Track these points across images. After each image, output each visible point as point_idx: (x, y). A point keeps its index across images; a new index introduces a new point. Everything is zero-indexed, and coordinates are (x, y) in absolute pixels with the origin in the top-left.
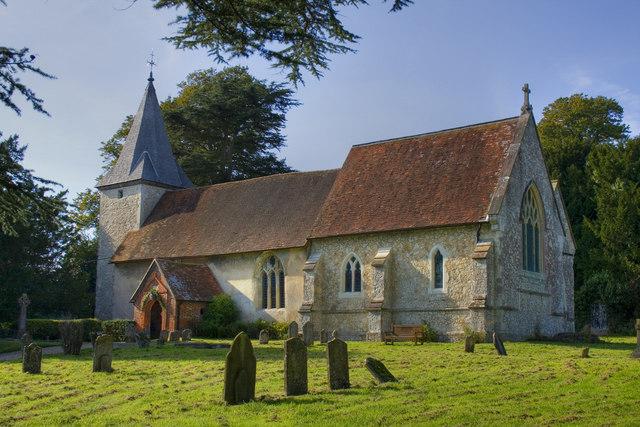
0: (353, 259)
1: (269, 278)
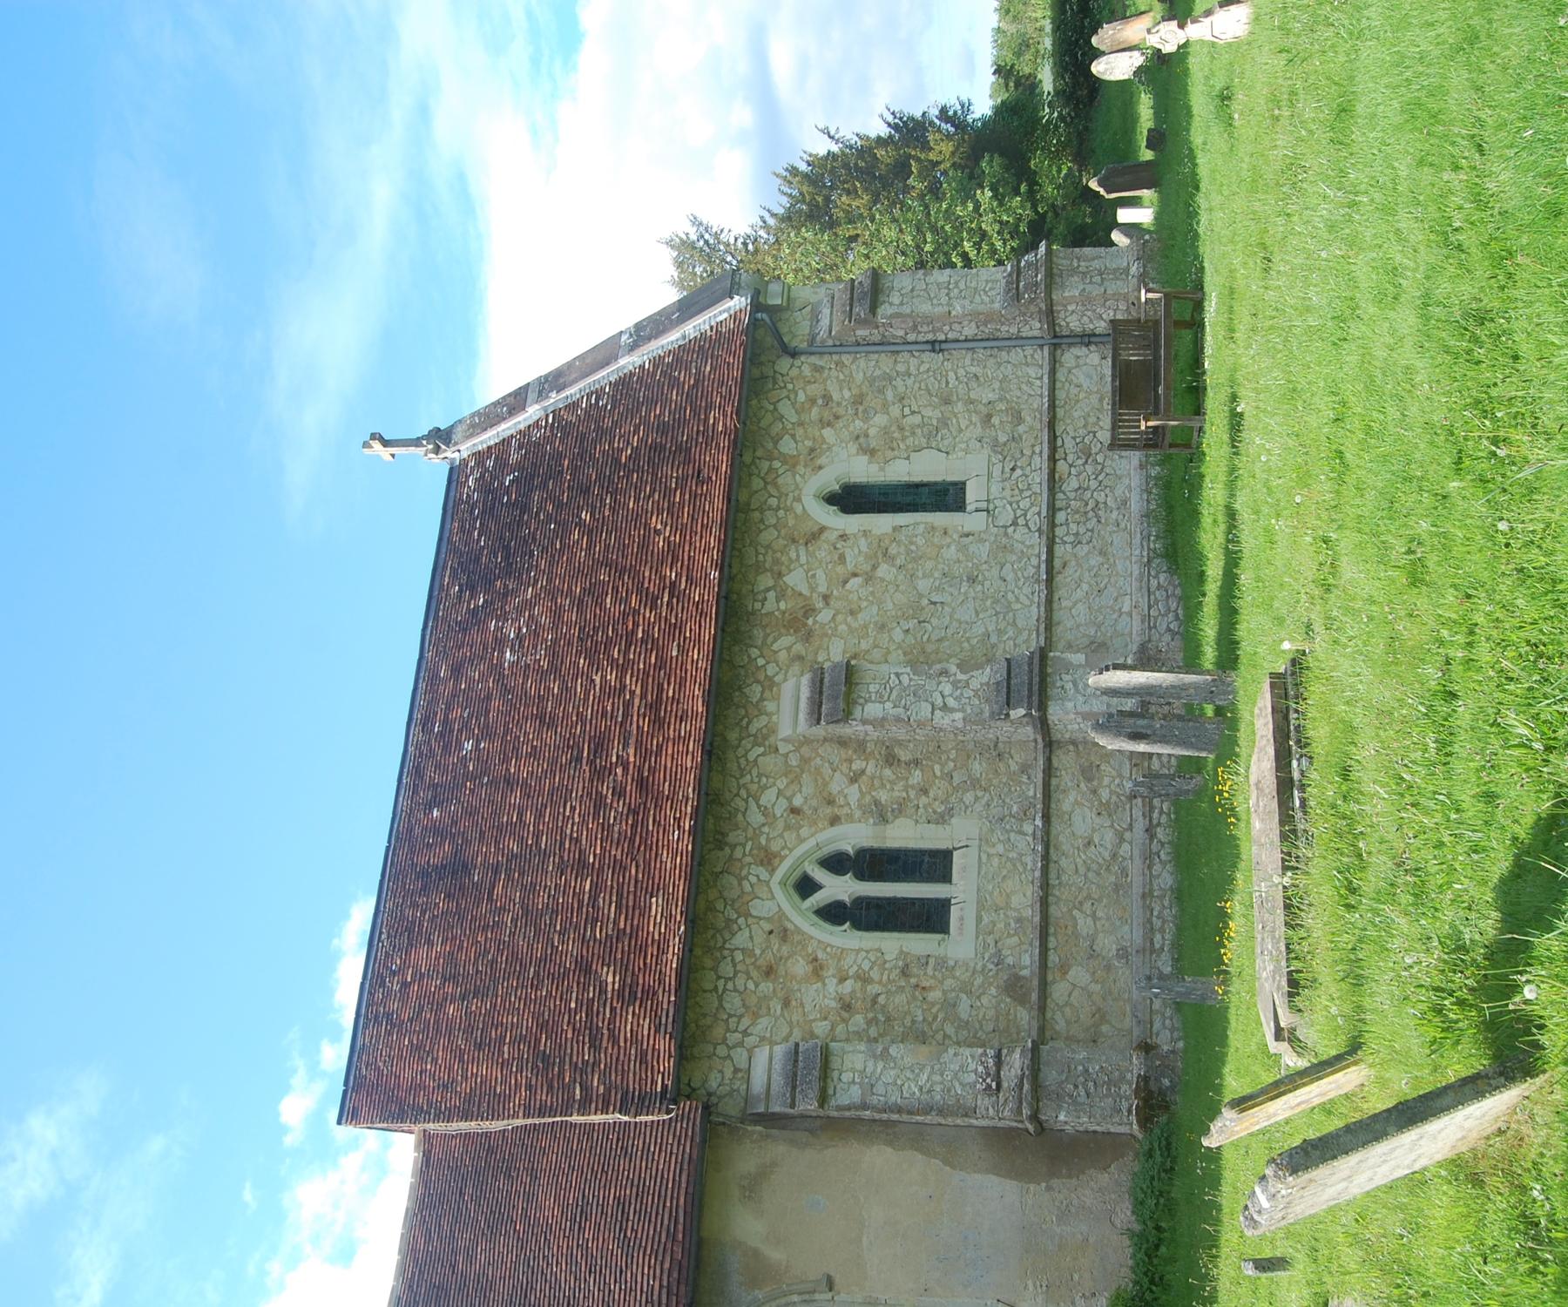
0: (806, 887)
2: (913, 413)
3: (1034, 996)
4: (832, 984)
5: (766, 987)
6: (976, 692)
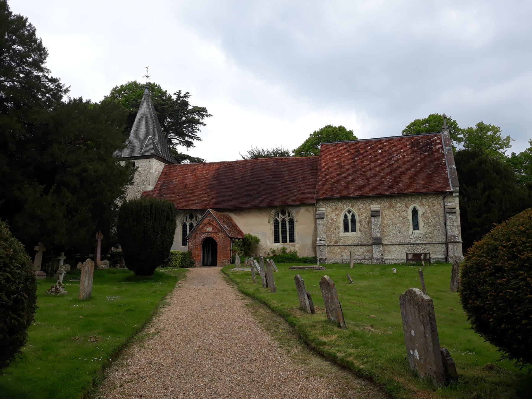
0: (349, 212)
1: (280, 224)
2: (431, 221)
3: (335, 244)
4: (335, 217)
5: (334, 208)
6: (377, 234)
